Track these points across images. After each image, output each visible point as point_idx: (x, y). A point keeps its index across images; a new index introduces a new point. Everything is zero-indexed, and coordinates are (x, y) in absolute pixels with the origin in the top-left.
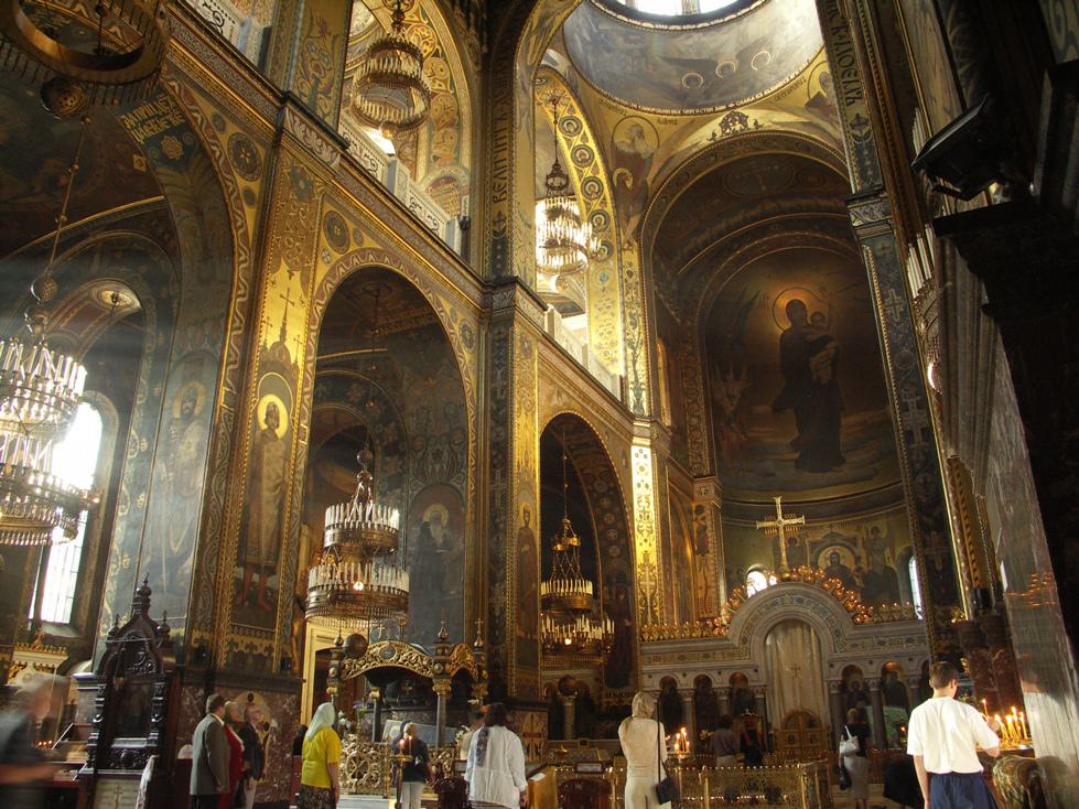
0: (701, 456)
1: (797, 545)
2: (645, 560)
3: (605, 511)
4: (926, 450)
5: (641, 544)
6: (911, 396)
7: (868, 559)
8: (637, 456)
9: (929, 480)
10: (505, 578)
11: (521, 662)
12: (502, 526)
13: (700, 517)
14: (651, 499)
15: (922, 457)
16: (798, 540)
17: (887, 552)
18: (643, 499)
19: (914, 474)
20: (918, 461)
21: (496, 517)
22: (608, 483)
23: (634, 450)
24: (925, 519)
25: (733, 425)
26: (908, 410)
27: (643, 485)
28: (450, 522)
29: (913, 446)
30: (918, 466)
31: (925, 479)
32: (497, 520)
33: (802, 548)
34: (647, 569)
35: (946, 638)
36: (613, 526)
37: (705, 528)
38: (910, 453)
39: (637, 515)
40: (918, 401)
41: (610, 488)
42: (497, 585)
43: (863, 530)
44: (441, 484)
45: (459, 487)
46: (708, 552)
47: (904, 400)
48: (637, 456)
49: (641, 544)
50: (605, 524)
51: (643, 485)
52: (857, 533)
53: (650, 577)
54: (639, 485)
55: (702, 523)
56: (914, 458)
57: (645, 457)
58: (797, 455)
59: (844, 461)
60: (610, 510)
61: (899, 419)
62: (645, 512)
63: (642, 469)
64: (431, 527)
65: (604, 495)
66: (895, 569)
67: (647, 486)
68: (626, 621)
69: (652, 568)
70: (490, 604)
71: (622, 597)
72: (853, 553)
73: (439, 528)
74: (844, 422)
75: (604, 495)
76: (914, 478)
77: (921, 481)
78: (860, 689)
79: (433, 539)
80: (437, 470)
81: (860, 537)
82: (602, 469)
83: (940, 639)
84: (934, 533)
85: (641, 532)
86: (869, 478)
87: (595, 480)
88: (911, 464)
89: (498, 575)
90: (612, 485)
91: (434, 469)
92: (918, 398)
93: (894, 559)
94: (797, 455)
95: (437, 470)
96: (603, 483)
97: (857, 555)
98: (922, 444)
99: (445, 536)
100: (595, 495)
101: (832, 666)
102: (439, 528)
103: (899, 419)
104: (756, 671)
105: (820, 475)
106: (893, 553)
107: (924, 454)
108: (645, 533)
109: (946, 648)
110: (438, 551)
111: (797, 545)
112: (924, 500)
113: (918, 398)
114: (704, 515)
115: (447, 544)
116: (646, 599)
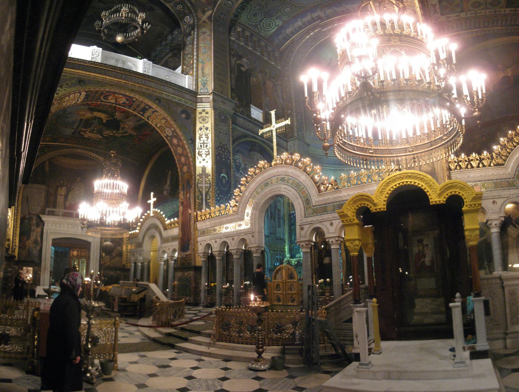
2: (203, 171)
11: (65, 213)
14: (210, 136)
34: (204, 177)
49: (200, 162)
53: (206, 181)
62: (204, 143)
68: (189, 210)
69: (207, 176)
101: (302, 229)
108: (204, 156)
116: (202, 195)
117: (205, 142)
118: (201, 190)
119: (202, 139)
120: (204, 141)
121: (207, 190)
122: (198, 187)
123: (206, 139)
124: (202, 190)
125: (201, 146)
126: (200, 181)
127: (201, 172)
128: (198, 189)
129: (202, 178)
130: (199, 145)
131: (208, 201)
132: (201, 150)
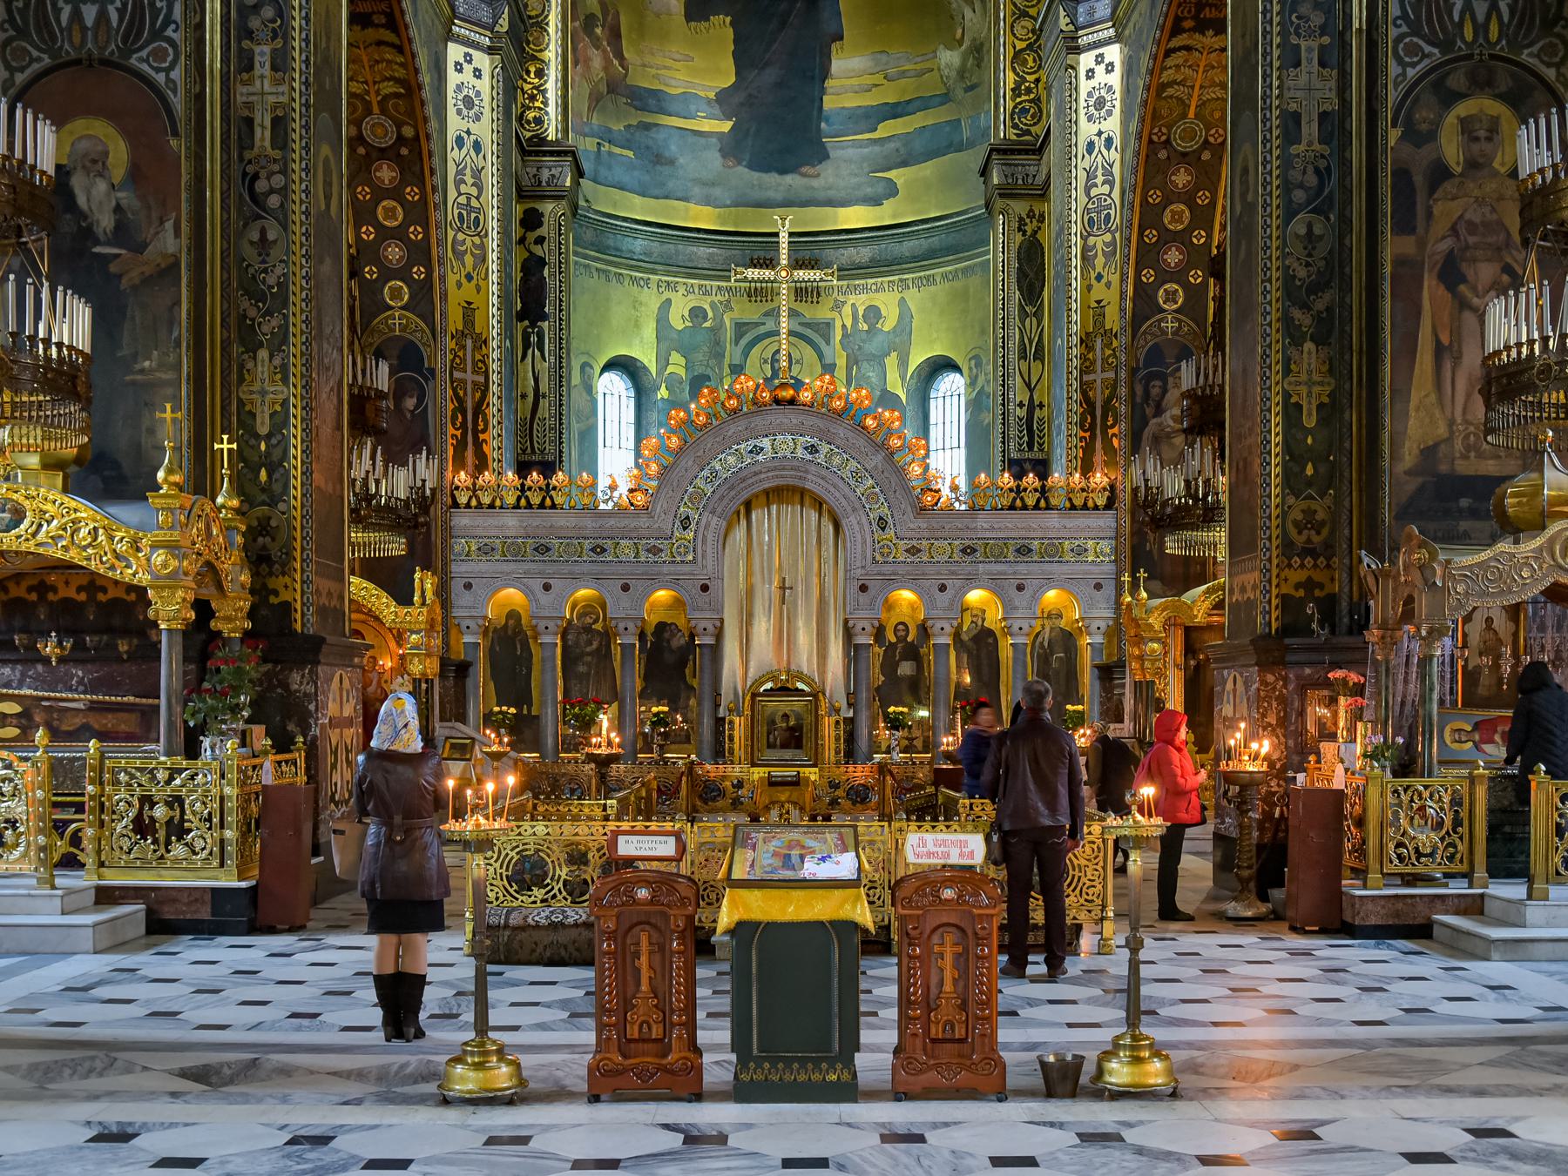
0: (544, 92)
1: (707, 324)
3: (380, 194)
4: (1322, 164)
5: (459, 285)
6: (1311, 34)
7: (849, 369)
8: (459, 68)
9: (1317, 230)
10: (285, 341)
12: (274, 201)
13: (531, 236)
15: (1312, 180)
16: (710, 314)
17: (891, 361)
18: (470, 180)
19: (1289, 213)
20: (1301, 186)
21: (256, 177)
22: (399, 125)
23: (455, 52)
24: (1297, 314)
25: (598, 31)
26: (1298, 64)
27: (469, 142)
28: (136, 174)
29: (1294, 149)
30: (1299, 196)
31: (1310, 226)
32: (261, 186)
33: (716, 330)
34: (469, 343)
35: (1302, 566)
36: (399, 234)
37: (542, 262)
38: (1287, 163)
39: (452, 213)
40: (1322, 48)
41: (401, 139)
42: (263, 354)
43: (847, 310)
44: (106, 62)
45: (161, 78)
46: (544, 317)
47: (1294, 40)
48: (459, 68)
50: (379, 227)
51: (469, 142)
52: (835, 314)
53: (475, 363)
54: (460, 142)
55: (538, 250)
56: (1295, 175)
57: (478, 73)
58: (726, 126)
59: (826, 157)
60: (396, 194)
61: (1276, 83)
63: (469, 103)
64: (77, 182)
65: (383, 153)
66: (903, 398)
67: (477, 146)
70: (241, 403)
71: (410, 403)
72: (821, 356)
73: (101, 186)
74: (837, 65)
75: (383, 153)
76: (1287, 222)
77: (1303, 231)
78: (909, 639)
79: (82, 215)
80: (89, 20)
81: (838, 324)
82: (389, 88)
83: (1290, 566)
84: (1309, 346)
85: (460, 256)
86: (876, 201)
87: (369, 112)
88: (1287, 187)
89: (265, 328)
90: (408, 132)
91: (77, 16)
92: (1326, 40)
93: (903, 378)
94: (726, 126)
95: (89, 20)
96: (388, 123)
97: (828, 361)
98: (1317, 146)
99: (118, 209)
100: (361, 151)
102: (101, 186)
103: (1276, 83)
104: (705, 588)
105: (772, 178)
106: (903, 363)
107: (1317, 171)
108: (469, 259)
109: (1297, 586)
110: (97, 249)
111: (707, 324)
112: (1302, 273)
113: (1326, 40)
114: (543, 231)
115: (123, 232)
117: (474, 203)
118: (461, 393)
119: (463, 188)
120: (469, 199)
121: (478, 395)
122: (452, 383)
123: (474, 192)
124: (465, 394)
125: (460, 215)
126: (458, 361)
127: (460, 328)
128: (454, 390)
129: (464, 347)
130: (456, 212)
131: (482, 436)
132: (460, 236)
